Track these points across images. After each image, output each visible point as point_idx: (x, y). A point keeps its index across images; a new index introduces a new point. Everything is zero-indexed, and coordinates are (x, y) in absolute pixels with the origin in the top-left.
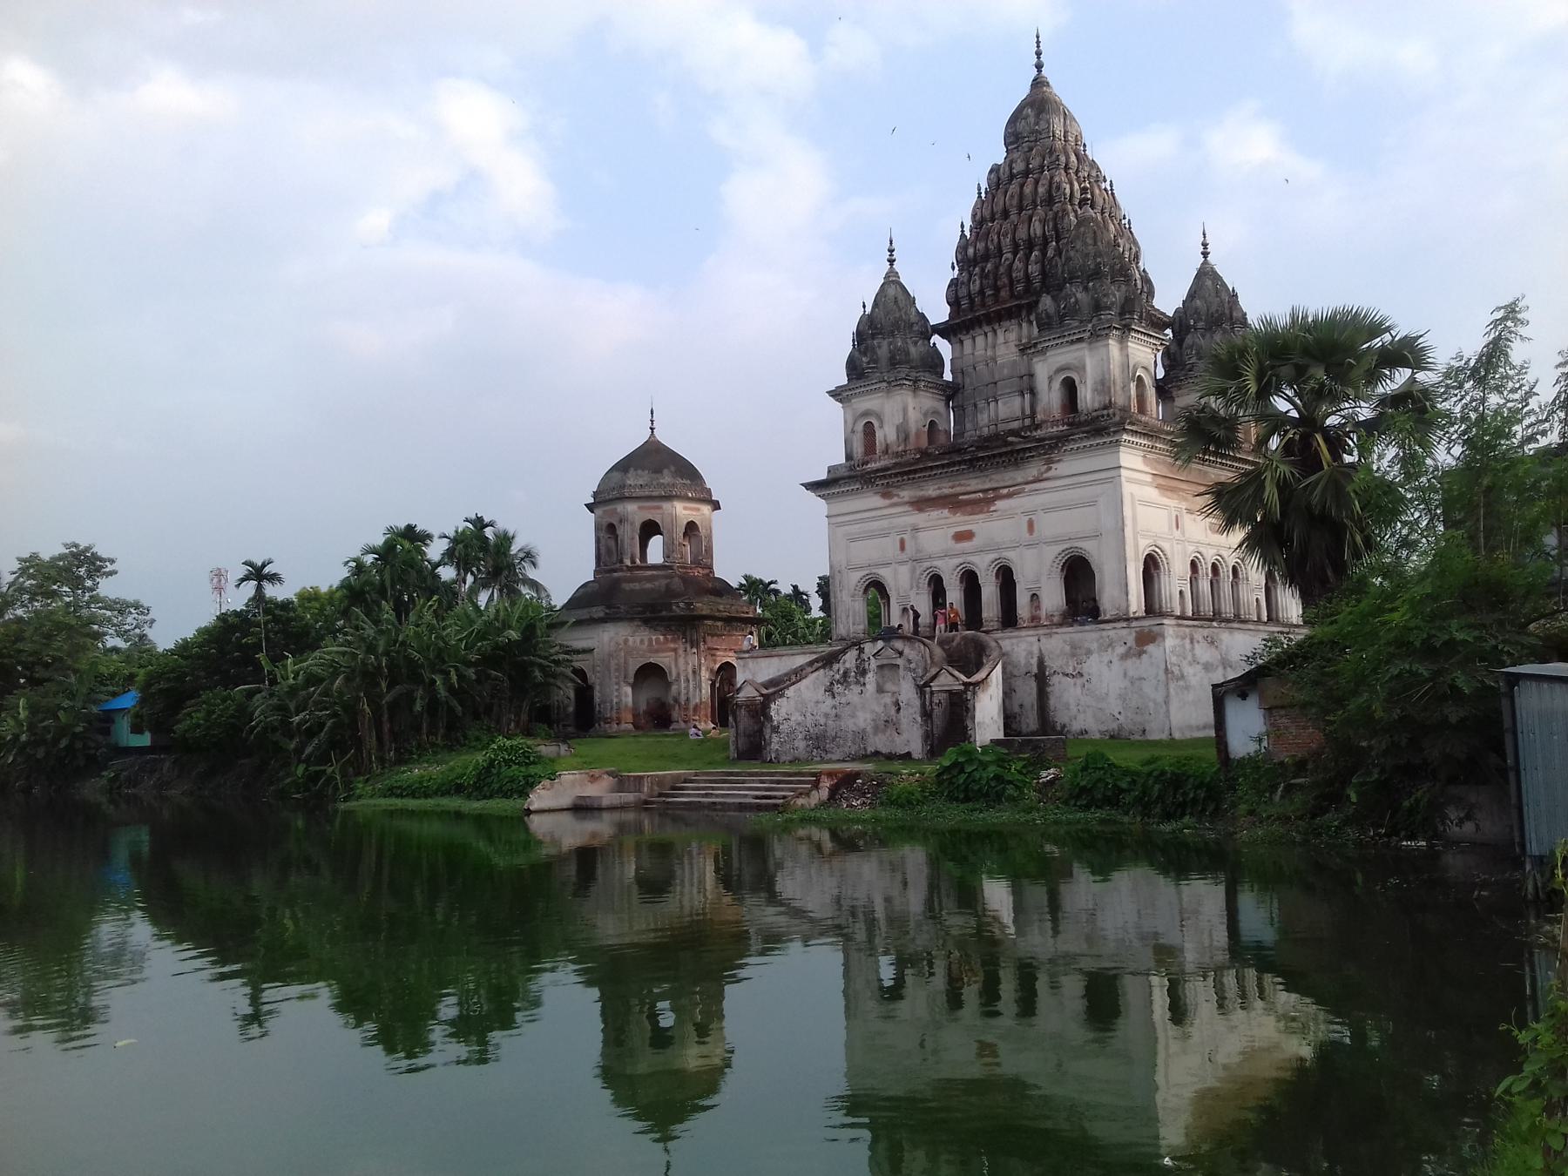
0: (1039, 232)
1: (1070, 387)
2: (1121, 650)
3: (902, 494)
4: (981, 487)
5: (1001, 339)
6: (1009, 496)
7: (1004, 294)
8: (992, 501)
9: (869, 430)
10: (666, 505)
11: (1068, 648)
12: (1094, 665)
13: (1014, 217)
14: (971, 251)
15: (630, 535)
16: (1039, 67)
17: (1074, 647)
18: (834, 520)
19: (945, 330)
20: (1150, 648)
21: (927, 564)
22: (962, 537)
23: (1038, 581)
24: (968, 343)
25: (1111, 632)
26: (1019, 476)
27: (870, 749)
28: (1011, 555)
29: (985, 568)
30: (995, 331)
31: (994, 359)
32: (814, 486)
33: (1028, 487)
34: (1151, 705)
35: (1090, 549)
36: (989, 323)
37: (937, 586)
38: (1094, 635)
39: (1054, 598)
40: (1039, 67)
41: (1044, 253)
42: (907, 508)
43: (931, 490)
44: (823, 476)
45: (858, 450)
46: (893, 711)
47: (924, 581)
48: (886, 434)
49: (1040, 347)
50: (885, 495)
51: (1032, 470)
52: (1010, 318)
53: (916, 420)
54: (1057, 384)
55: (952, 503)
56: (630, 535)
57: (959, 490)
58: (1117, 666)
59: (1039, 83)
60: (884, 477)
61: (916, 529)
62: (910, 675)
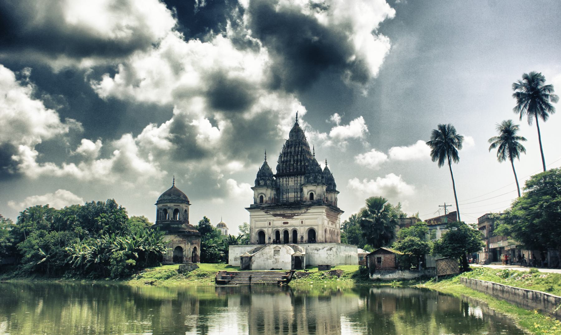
1: (312, 195)
5: (290, 180)
7: (291, 171)
9: (262, 198)
10: (181, 205)
12: (321, 252)
14: (283, 159)
15: (170, 212)
16: (297, 120)
19: (274, 176)
22: (284, 223)
24: (281, 180)
25: (324, 245)
26: (300, 212)
29: (290, 229)
32: (246, 209)
35: (315, 228)
37: (277, 233)
39: (306, 238)
40: (297, 120)
41: (301, 164)
43: (278, 213)
44: (249, 207)
45: (258, 201)
50: (266, 212)
51: (303, 211)
52: (293, 176)
53: (273, 196)
54: (309, 194)
55: (283, 216)
56: (170, 212)
58: (326, 252)
61: (273, 221)
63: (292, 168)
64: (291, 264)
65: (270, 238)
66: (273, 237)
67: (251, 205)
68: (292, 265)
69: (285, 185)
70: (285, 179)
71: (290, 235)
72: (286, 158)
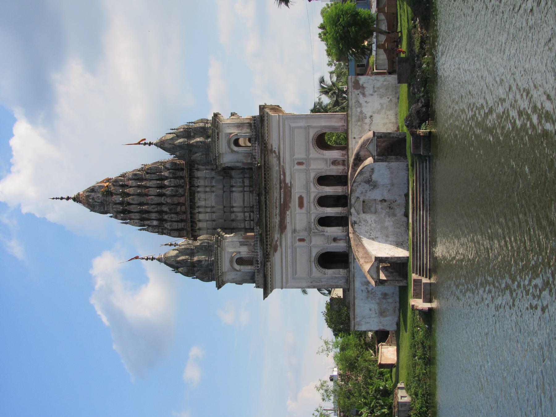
0: (155, 182)
2: (361, 96)
3: (276, 239)
4: (278, 191)
5: (202, 203)
6: (284, 174)
7: (182, 200)
8: (286, 185)
11: (359, 123)
13: (144, 199)
14: (155, 223)
16: (68, 198)
17: (359, 120)
18: (284, 284)
20: (361, 83)
21: (313, 226)
22: (301, 205)
23: (326, 160)
27: (405, 219)
28: (312, 175)
30: (198, 207)
31: (213, 207)
32: (266, 295)
33: (282, 164)
34: (385, 83)
36: (195, 209)
38: (354, 110)
41: (166, 178)
42: (283, 236)
43: (277, 220)
44: (261, 291)
45: (248, 268)
46: (385, 204)
47: (321, 228)
48: (244, 251)
49: (217, 155)
50: (276, 250)
51: (273, 161)
55: (284, 207)
57: (278, 204)
58: (369, 99)
59: (76, 199)
60: (267, 245)
61: (294, 231)
62: (369, 194)
63: (176, 200)
64: (394, 164)
65: (335, 240)
66: (334, 231)
67: (258, 287)
68: (397, 160)
69: (214, 216)
70: (201, 217)
71: (329, 190)
72: (154, 216)
